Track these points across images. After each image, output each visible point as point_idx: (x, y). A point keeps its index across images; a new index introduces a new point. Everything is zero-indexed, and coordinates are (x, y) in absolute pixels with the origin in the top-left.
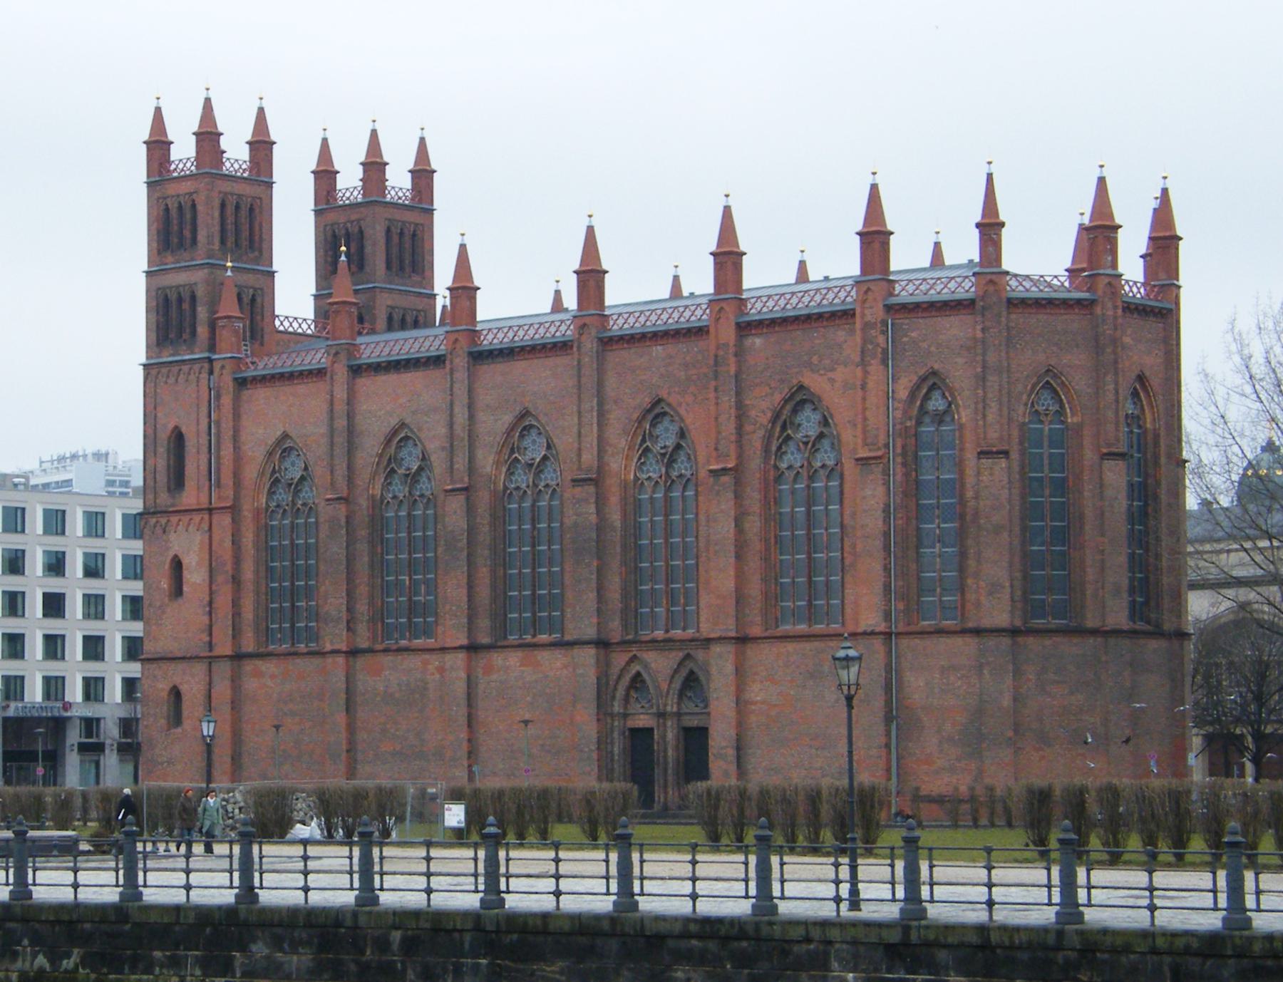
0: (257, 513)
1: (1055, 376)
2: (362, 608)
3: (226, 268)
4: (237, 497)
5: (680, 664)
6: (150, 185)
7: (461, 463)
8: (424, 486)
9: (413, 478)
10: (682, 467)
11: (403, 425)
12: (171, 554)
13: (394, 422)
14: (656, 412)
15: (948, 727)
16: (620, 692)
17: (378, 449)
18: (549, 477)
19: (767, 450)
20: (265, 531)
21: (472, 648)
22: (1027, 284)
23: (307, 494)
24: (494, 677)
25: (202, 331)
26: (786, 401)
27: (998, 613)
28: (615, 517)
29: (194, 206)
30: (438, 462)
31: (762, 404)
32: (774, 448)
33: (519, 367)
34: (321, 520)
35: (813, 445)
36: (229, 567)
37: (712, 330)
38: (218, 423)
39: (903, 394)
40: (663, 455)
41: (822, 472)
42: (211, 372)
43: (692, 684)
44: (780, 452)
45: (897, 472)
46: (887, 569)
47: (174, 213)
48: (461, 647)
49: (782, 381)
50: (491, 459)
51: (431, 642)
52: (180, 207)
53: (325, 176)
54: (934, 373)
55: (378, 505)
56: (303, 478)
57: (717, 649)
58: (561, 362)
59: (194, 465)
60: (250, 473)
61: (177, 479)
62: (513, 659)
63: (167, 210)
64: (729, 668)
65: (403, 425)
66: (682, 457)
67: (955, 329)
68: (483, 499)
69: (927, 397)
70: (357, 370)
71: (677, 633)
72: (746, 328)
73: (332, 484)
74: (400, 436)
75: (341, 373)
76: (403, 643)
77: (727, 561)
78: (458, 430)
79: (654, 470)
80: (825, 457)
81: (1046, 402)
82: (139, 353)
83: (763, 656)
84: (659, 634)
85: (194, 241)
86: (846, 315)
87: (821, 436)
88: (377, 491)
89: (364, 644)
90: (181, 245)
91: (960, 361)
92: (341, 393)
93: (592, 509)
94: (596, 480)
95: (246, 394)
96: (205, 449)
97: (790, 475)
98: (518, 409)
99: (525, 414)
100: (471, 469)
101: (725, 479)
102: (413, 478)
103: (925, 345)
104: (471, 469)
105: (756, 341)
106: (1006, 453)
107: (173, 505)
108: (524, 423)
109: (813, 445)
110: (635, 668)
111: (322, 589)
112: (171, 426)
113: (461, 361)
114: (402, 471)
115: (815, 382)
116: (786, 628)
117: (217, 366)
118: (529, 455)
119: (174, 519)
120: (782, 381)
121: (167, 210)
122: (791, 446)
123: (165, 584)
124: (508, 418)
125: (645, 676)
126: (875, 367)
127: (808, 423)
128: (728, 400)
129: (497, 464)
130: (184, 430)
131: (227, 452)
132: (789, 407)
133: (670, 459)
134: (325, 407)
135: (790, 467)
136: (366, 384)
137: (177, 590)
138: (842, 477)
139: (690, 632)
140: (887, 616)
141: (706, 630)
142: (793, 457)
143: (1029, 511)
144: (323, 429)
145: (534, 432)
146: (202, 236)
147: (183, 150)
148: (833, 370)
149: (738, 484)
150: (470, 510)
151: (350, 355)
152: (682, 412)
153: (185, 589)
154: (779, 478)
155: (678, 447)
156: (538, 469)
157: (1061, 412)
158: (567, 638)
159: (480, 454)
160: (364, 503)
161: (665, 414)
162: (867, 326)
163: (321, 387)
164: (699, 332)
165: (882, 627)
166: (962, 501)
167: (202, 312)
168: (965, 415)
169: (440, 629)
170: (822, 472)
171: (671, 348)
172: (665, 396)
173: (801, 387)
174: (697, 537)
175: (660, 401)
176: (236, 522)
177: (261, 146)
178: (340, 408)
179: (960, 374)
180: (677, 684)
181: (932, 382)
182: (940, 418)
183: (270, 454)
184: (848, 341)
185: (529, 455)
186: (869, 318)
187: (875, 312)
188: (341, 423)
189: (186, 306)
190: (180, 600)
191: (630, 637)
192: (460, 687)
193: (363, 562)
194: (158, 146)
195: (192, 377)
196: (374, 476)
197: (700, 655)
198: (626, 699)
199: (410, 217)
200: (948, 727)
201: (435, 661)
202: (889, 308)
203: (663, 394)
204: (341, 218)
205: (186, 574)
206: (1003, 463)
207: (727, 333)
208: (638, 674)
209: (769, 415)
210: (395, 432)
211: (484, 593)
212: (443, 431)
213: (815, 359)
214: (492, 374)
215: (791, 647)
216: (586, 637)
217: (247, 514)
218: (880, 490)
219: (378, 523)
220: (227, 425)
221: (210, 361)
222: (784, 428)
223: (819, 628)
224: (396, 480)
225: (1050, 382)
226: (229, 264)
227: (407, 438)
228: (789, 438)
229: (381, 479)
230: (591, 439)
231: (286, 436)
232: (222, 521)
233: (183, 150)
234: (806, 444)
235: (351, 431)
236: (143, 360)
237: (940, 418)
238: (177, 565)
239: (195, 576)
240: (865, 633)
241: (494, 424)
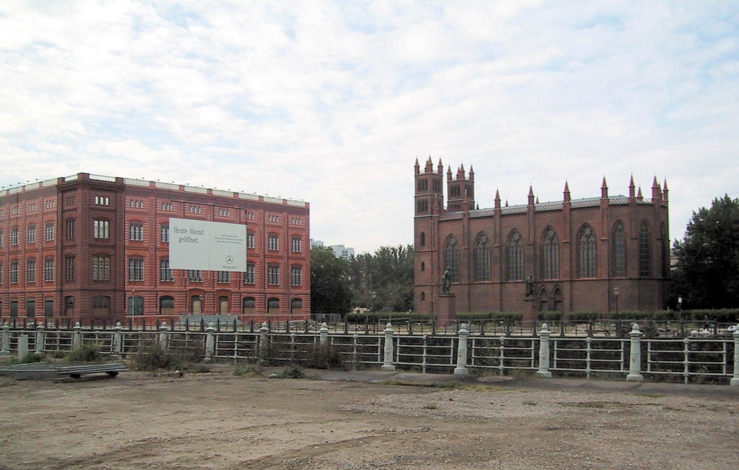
0: (443, 251)
1: (647, 221)
2: (472, 274)
3: (435, 195)
4: (439, 248)
5: (554, 288)
6: (415, 176)
7: (498, 240)
8: (487, 246)
9: (484, 244)
10: (555, 241)
11: (482, 232)
12: (421, 262)
13: (479, 231)
14: (548, 229)
16: (539, 293)
17: (475, 237)
18: (520, 243)
19: (577, 238)
20: (445, 256)
21: (501, 283)
23: (456, 247)
25: (429, 210)
26: (582, 226)
27: (636, 276)
28: (538, 253)
29: (427, 181)
30: (492, 240)
31: (577, 227)
33: (513, 218)
35: (588, 236)
36: (437, 264)
38: (434, 231)
39: (612, 225)
41: (591, 243)
42: (432, 219)
43: (557, 291)
44: (580, 238)
45: (611, 242)
46: (609, 265)
47: (421, 183)
48: (498, 283)
50: (505, 239)
52: (423, 181)
53: (450, 174)
54: (619, 220)
55: (475, 250)
56: (455, 244)
57: (564, 283)
58: (524, 217)
59: (427, 240)
60: (442, 242)
61: (423, 243)
62: (511, 285)
63: (419, 182)
64: (568, 288)
65: (482, 232)
66: (555, 239)
67: (624, 210)
68: (504, 249)
69: (617, 226)
70: (470, 219)
72: (572, 210)
73: (464, 245)
74: (481, 234)
75: (466, 220)
76: (482, 282)
77: (568, 263)
78: (497, 233)
79: (548, 242)
80: (592, 239)
81: (644, 228)
82: (413, 215)
83: (576, 285)
84: (550, 280)
85: (427, 189)
86: (598, 207)
87: (591, 234)
88: (475, 247)
89: (472, 282)
90: (423, 190)
94: (534, 244)
95: (441, 224)
96: (430, 237)
99: (514, 229)
100: (501, 241)
101: (567, 244)
102: (484, 244)
104: (501, 241)
105: (574, 213)
106: (636, 239)
107: (423, 249)
108: (513, 232)
109: (588, 236)
110: (543, 287)
112: (421, 233)
113: (498, 217)
115: (589, 222)
116: (582, 279)
117: (433, 218)
119: (422, 253)
121: (419, 182)
122: (583, 237)
123: (420, 268)
124: (509, 230)
125: (546, 289)
126: (605, 218)
128: (568, 226)
129: (507, 240)
130: (424, 232)
131: (436, 238)
132: (582, 228)
133: (552, 239)
136: (472, 222)
137: (423, 269)
140: (609, 277)
141: (562, 278)
142: (584, 239)
143: (641, 252)
146: (429, 188)
147: (422, 170)
149: (570, 245)
150: (501, 251)
151: (469, 215)
152: (556, 229)
153: (425, 269)
154: (580, 244)
156: (517, 241)
157: (647, 230)
159: (502, 238)
160: (472, 250)
162: (603, 209)
164: (560, 210)
165: (607, 278)
166: (626, 250)
167: (429, 206)
168: (626, 230)
170: (591, 243)
173: (586, 223)
176: (439, 254)
177: (440, 167)
179: (626, 221)
180: (554, 291)
182: (620, 230)
183: (447, 238)
184: (598, 213)
186: (604, 207)
187: (605, 206)
188: (466, 231)
189: (425, 204)
190: (424, 272)
192: (498, 291)
193: (472, 265)
194: (417, 167)
195: (427, 220)
196: (474, 243)
197: (560, 284)
198: (541, 294)
199: (470, 183)
201: (491, 286)
202: (609, 205)
203: (551, 224)
204: (454, 184)
205: (425, 266)
206: (636, 241)
207: (568, 211)
210: (480, 233)
211: (504, 270)
214: (505, 219)
217: (441, 252)
218: (607, 247)
219: (475, 255)
220: (436, 231)
221: (432, 217)
224: (480, 244)
225: (645, 223)
226: (436, 194)
227: (483, 234)
228: (582, 235)
229: (476, 243)
230: (532, 234)
231: (451, 234)
232: (435, 254)
233: (422, 170)
235: (469, 233)
236: (414, 216)
237: (620, 230)
238: (423, 264)
239: (428, 266)
241: (507, 231)
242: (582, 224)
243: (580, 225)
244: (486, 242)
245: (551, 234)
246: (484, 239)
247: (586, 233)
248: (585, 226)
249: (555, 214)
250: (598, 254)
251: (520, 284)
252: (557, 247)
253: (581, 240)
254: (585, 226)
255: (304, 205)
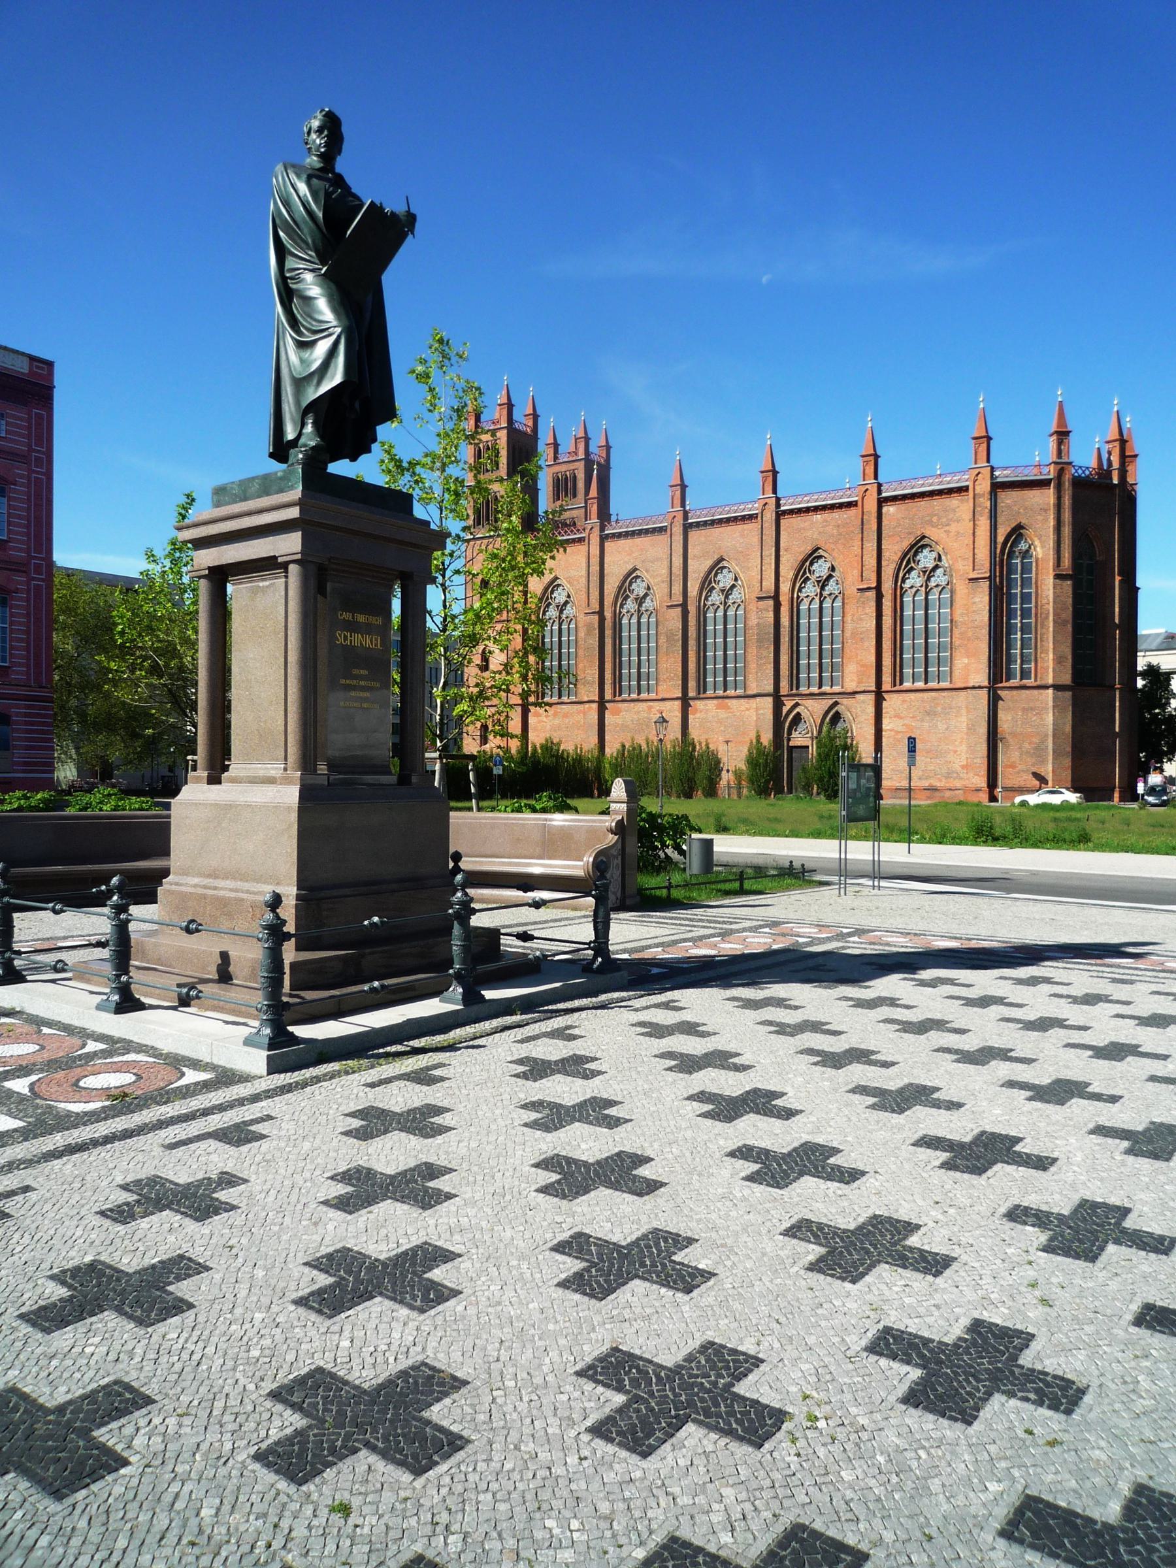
7: (677, 588)
8: (648, 603)
9: (640, 601)
10: (831, 587)
11: (635, 569)
13: (630, 567)
14: (813, 556)
15: (1026, 745)
22: (1080, 471)
23: (569, 611)
24: (698, 715)
31: (893, 550)
32: (901, 575)
33: (717, 531)
34: (580, 625)
37: (860, 503)
40: (818, 582)
49: (910, 533)
51: (653, 695)
57: (861, 697)
66: (832, 582)
71: (826, 688)
74: (631, 576)
80: (939, 578)
84: (815, 689)
87: (936, 567)
91: (1040, 518)
92: (595, 550)
93: (771, 614)
97: (912, 592)
98: (716, 557)
99: (721, 559)
103: (1016, 508)
108: (718, 566)
111: (581, 666)
113: (678, 529)
114: (632, 597)
118: (721, 585)
120: (910, 533)
122: (914, 574)
124: (709, 563)
127: (926, 559)
128: (871, 546)
134: (584, 561)
135: (912, 587)
138: (952, 592)
139: (837, 689)
141: (850, 686)
144: (584, 572)
145: (725, 571)
148: (948, 525)
152: (835, 554)
155: (830, 577)
158: (750, 692)
161: (820, 557)
163: (583, 548)
169: (660, 688)
170: (936, 591)
171: (828, 515)
172: (822, 546)
174: (843, 631)
175: (819, 548)
178: (595, 561)
181: (1017, 532)
184: (961, 507)
185: (721, 585)
187: (984, 486)
188: (595, 568)
191: (794, 691)
197: (845, 701)
200: (1026, 745)
204: (563, 468)
207: (871, 504)
208: (798, 714)
209: (899, 554)
212: (664, 571)
213: (935, 519)
215: (912, 696)
216: (766, 692)
222: (908, 562)
223: (931, 685)
234: (924, 572)
240: (974, 688)
241: (698, 568)
242: (911, 540)
243: (906, 544)
244: (646, 595)
245: (820, 569)
246: (639, 589)
247: (921, 565)
248: (919, 545)
249: (836, 515)
250: (957, 618)
251: (734, 701)
252: (838, 604)
253: (907, 585)
254: (919, 545)
255: (21, 367)
